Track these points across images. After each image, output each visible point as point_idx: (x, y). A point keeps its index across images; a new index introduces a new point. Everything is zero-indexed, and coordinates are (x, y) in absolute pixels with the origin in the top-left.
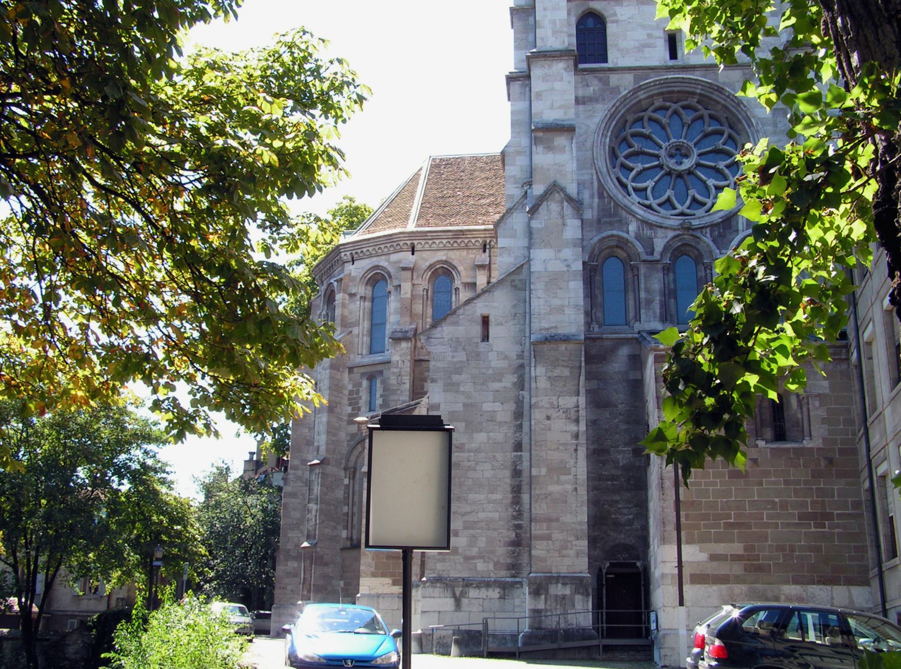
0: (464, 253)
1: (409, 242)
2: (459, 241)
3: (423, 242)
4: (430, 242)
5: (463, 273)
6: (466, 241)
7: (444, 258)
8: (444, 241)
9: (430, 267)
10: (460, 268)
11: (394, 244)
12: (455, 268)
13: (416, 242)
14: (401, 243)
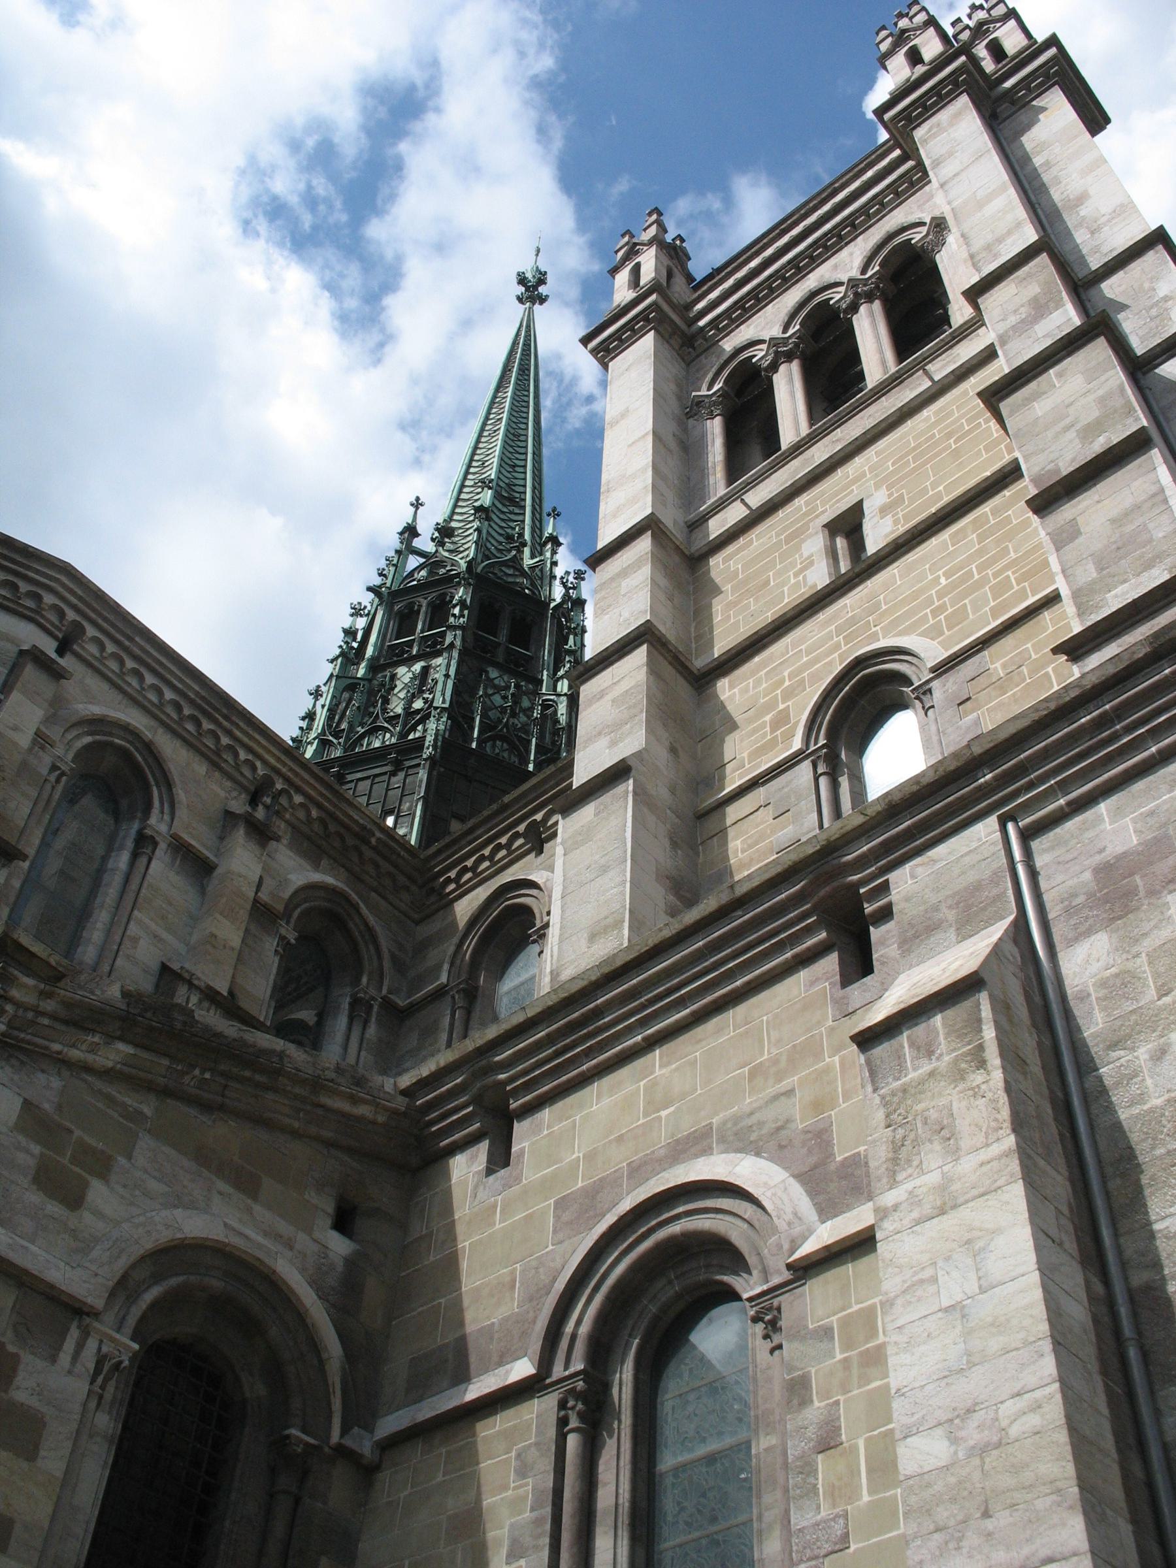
0: (201, 768)
1: (71, 615)
2: (207, 725)
3: (110, 648)
4: (130, 664)
5: (182, 813)
6: (225, 740)
7: (148, 735)
8: (169, 695)
9: (96, 724)
10: (180, 794)
11: (24, 587)
12: (167, 783)
13: (91, 631)
14: (49, 599)
